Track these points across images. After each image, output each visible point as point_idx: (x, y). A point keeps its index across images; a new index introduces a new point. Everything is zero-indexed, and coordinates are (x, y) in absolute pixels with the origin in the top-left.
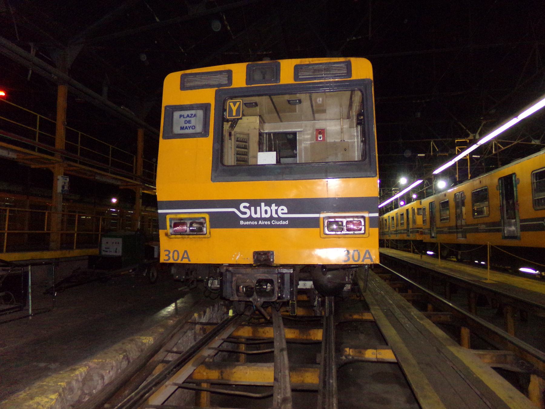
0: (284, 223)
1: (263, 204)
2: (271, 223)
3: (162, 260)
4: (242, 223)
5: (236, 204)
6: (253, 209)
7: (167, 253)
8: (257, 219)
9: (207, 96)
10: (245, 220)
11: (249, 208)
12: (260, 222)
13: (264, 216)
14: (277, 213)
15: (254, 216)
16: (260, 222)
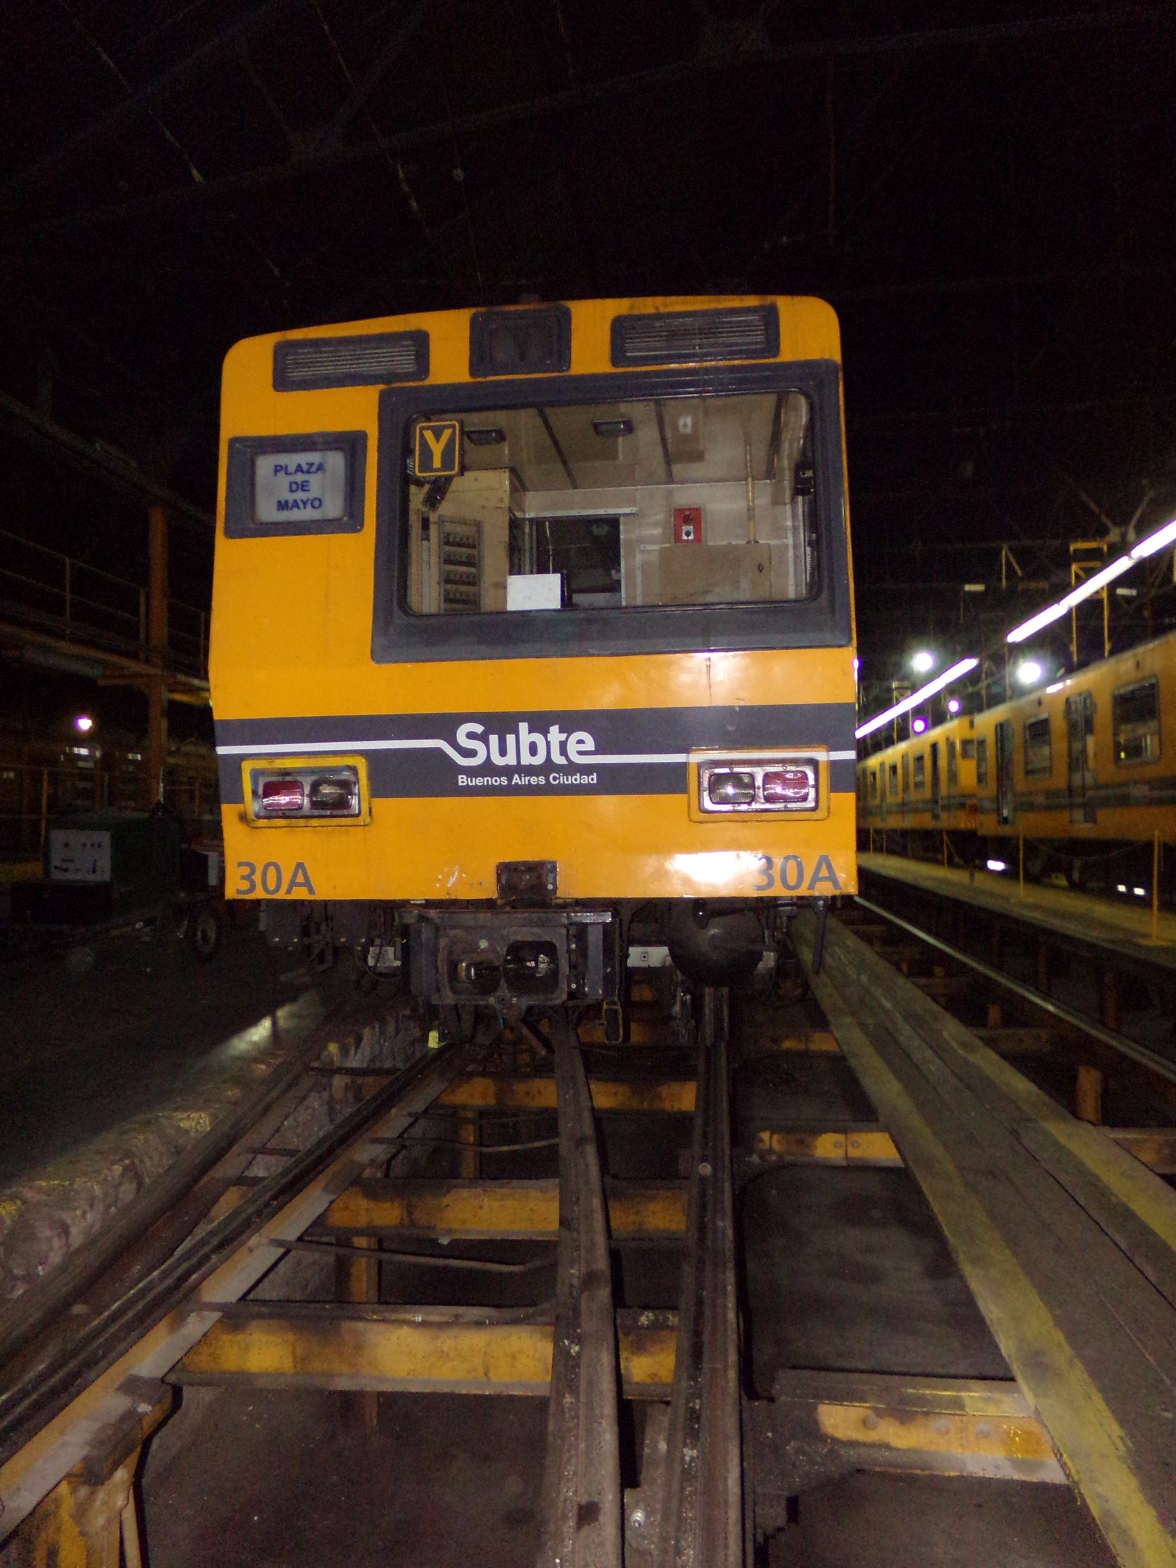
0: (585, 780)
1: (523, 727)
2: (548, 782)
3: (230, 893)
4: (462, 780)
5: (444, 725)
6: (494, 739)
7: (246, 871)
8: (508, 771)
9: (355, 409)
11: (483, 738)
12: (516, 779)
13: (527, 759)
15: (498, 760)
16: (516, 779)
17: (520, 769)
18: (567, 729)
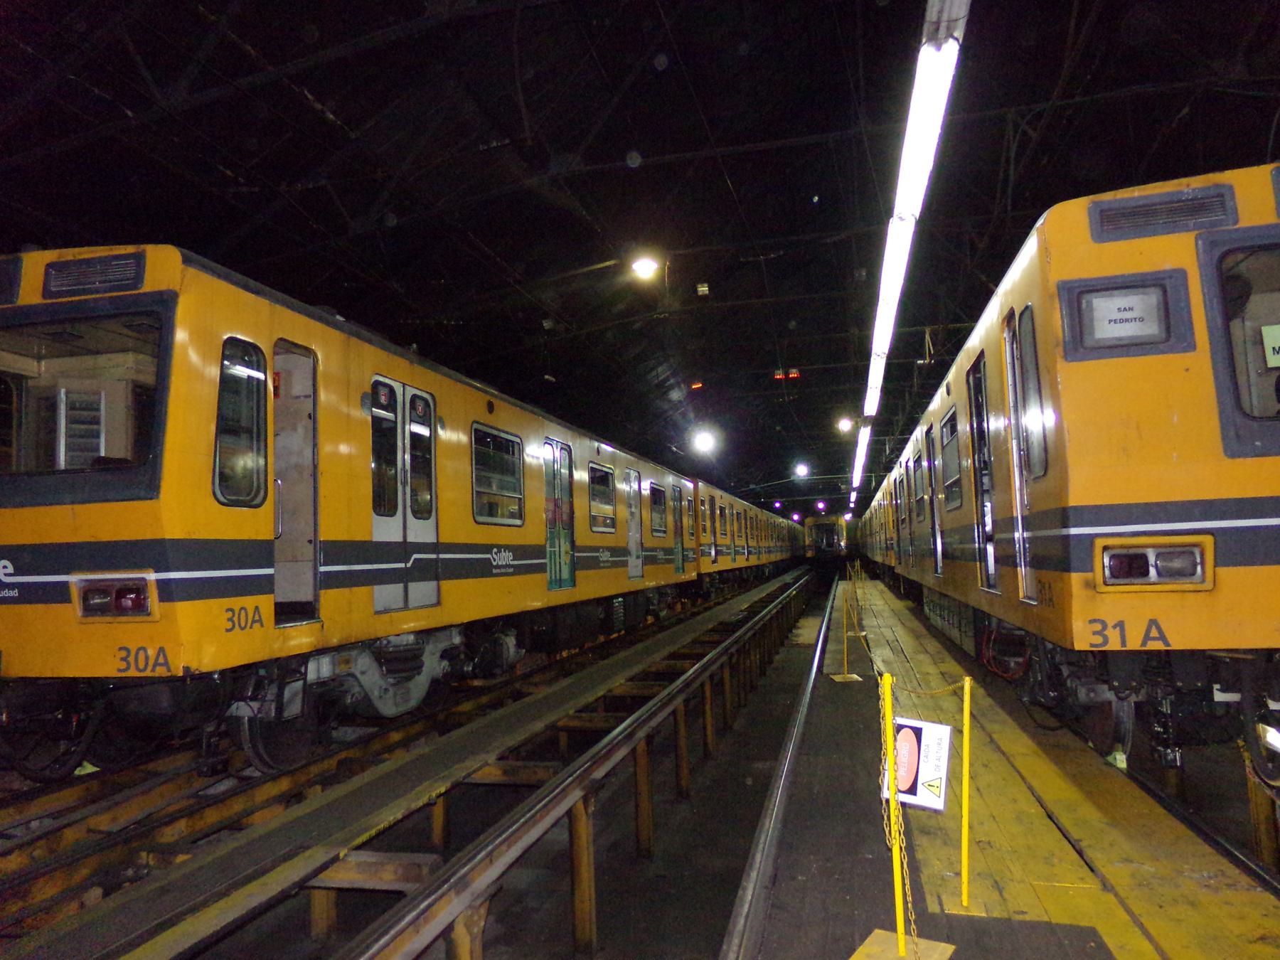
3: (1081, 644)
9: (1176, 251)
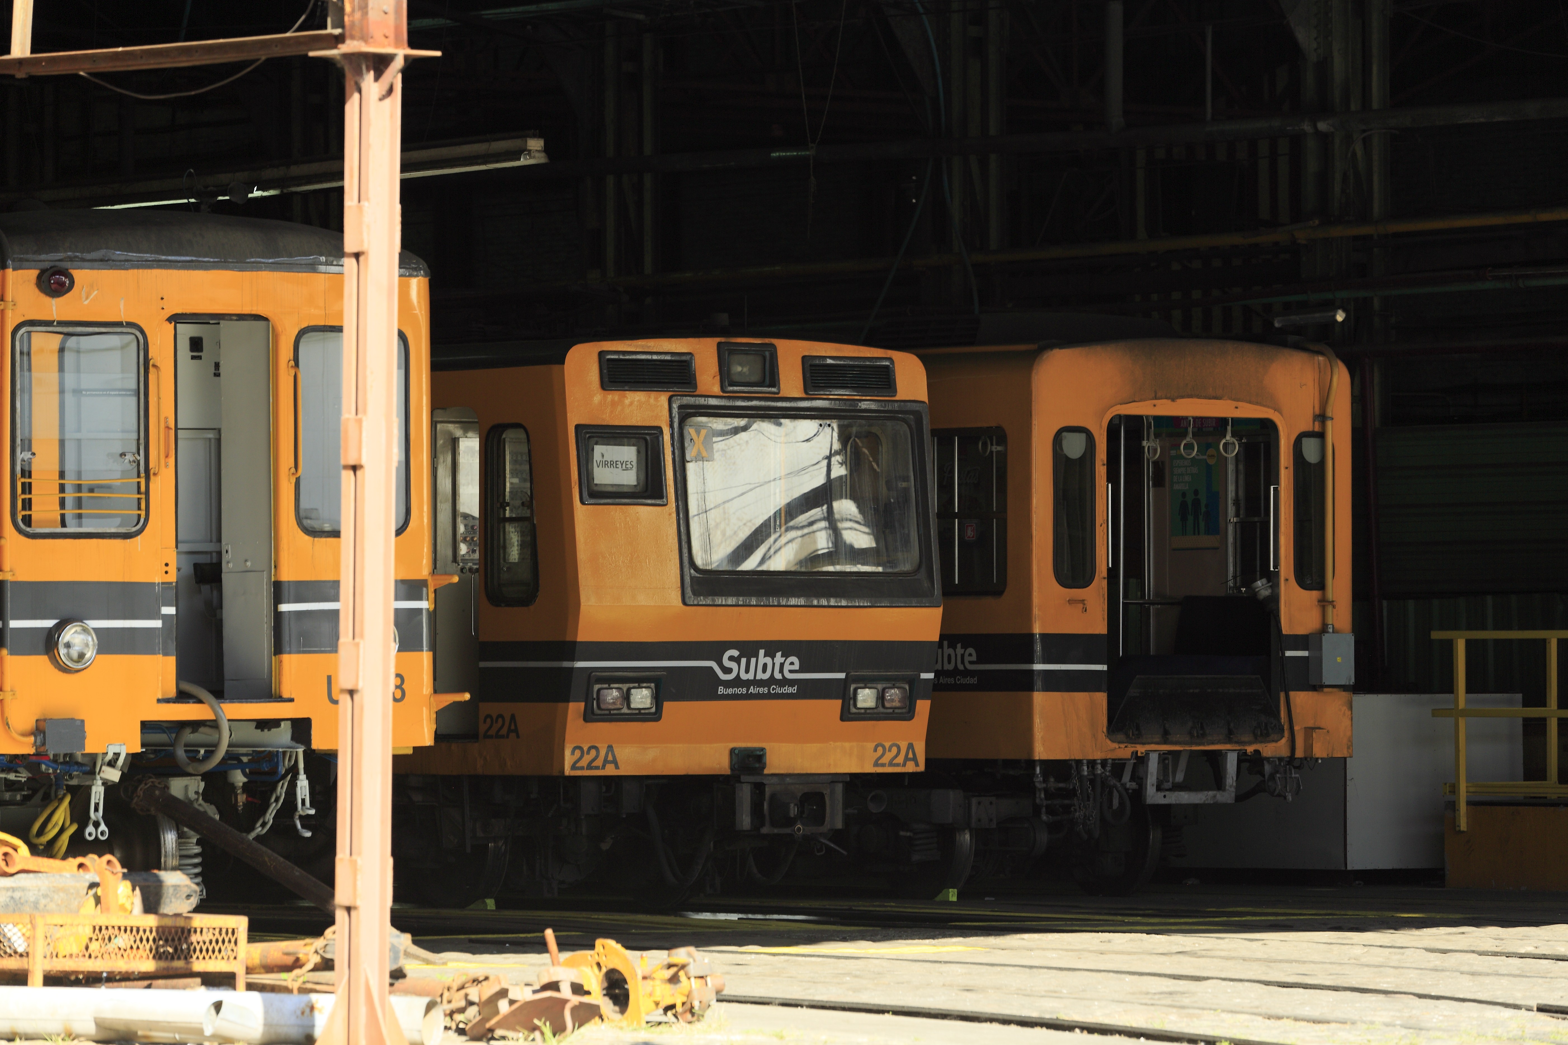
1: (762, 652)
4: (721, 690)
5: (714, 650)
6: (744, 661)
8: (748, 683)
10: (727, 684)
11: (737, 660)
12: (752, 690)
13: (760, 676)
14: (781, 671)
15: (744, 676)
17: (756, 683)
18: (786, 655)
